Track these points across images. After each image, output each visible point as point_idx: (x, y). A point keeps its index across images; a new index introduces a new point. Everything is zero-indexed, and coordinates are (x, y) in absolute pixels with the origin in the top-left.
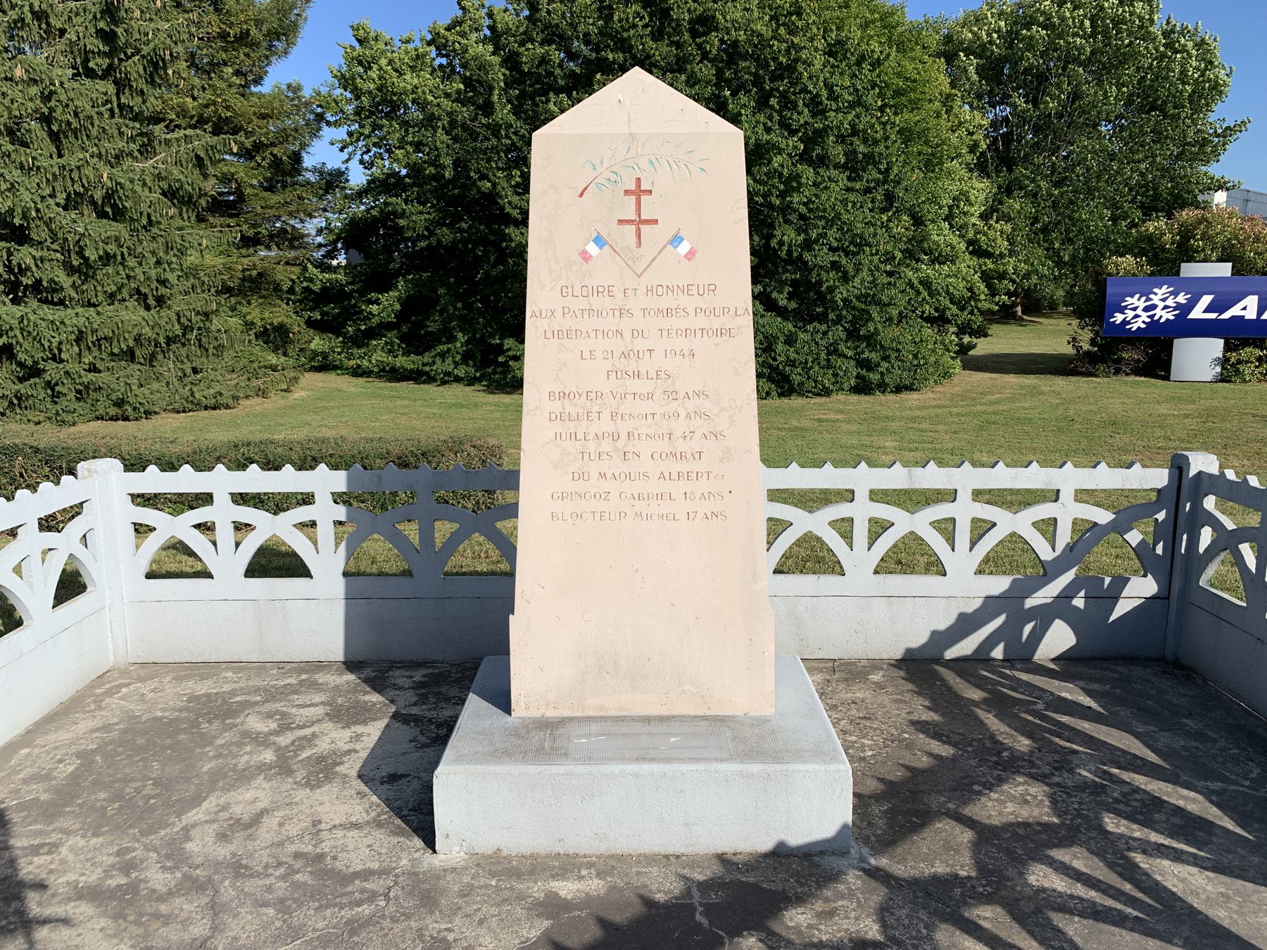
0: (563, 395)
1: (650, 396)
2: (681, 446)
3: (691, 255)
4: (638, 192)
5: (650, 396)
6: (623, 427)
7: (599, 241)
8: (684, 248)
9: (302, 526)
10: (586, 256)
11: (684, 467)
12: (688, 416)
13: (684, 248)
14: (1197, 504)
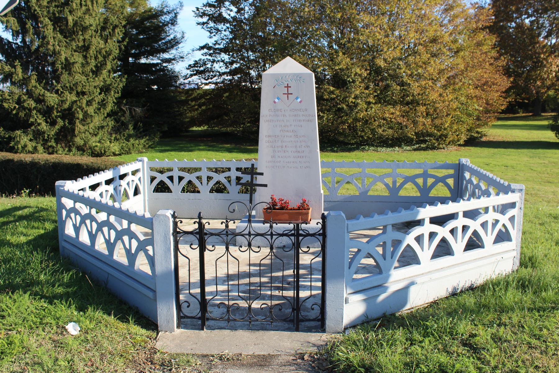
0: (269, 136)
1: (291, 137)
2: (299, 149)
3: (300, 102)
4: (288, 87)
5: (291, 137)
6: (284, 144)
7: (278, 98)
8: (299, 100)
9: (198, 178)
10: (275, 102)
11: (299, 155)
12: (300, 142)
13: (299, 100)
14: (463, 173)
